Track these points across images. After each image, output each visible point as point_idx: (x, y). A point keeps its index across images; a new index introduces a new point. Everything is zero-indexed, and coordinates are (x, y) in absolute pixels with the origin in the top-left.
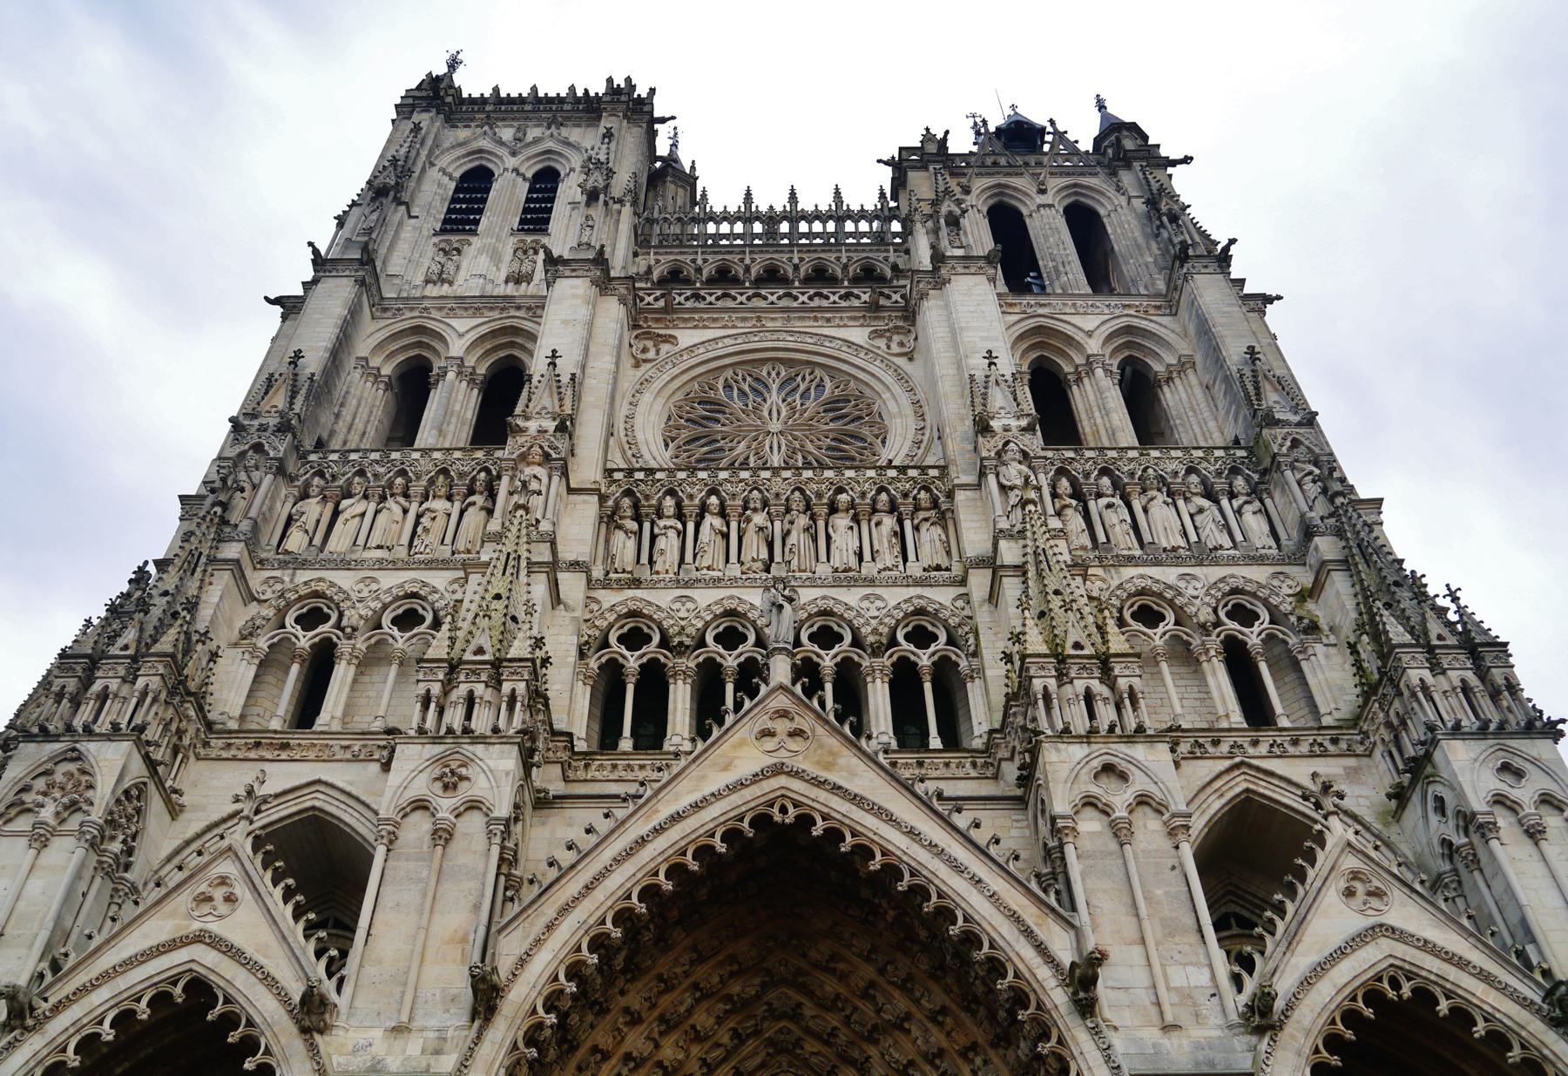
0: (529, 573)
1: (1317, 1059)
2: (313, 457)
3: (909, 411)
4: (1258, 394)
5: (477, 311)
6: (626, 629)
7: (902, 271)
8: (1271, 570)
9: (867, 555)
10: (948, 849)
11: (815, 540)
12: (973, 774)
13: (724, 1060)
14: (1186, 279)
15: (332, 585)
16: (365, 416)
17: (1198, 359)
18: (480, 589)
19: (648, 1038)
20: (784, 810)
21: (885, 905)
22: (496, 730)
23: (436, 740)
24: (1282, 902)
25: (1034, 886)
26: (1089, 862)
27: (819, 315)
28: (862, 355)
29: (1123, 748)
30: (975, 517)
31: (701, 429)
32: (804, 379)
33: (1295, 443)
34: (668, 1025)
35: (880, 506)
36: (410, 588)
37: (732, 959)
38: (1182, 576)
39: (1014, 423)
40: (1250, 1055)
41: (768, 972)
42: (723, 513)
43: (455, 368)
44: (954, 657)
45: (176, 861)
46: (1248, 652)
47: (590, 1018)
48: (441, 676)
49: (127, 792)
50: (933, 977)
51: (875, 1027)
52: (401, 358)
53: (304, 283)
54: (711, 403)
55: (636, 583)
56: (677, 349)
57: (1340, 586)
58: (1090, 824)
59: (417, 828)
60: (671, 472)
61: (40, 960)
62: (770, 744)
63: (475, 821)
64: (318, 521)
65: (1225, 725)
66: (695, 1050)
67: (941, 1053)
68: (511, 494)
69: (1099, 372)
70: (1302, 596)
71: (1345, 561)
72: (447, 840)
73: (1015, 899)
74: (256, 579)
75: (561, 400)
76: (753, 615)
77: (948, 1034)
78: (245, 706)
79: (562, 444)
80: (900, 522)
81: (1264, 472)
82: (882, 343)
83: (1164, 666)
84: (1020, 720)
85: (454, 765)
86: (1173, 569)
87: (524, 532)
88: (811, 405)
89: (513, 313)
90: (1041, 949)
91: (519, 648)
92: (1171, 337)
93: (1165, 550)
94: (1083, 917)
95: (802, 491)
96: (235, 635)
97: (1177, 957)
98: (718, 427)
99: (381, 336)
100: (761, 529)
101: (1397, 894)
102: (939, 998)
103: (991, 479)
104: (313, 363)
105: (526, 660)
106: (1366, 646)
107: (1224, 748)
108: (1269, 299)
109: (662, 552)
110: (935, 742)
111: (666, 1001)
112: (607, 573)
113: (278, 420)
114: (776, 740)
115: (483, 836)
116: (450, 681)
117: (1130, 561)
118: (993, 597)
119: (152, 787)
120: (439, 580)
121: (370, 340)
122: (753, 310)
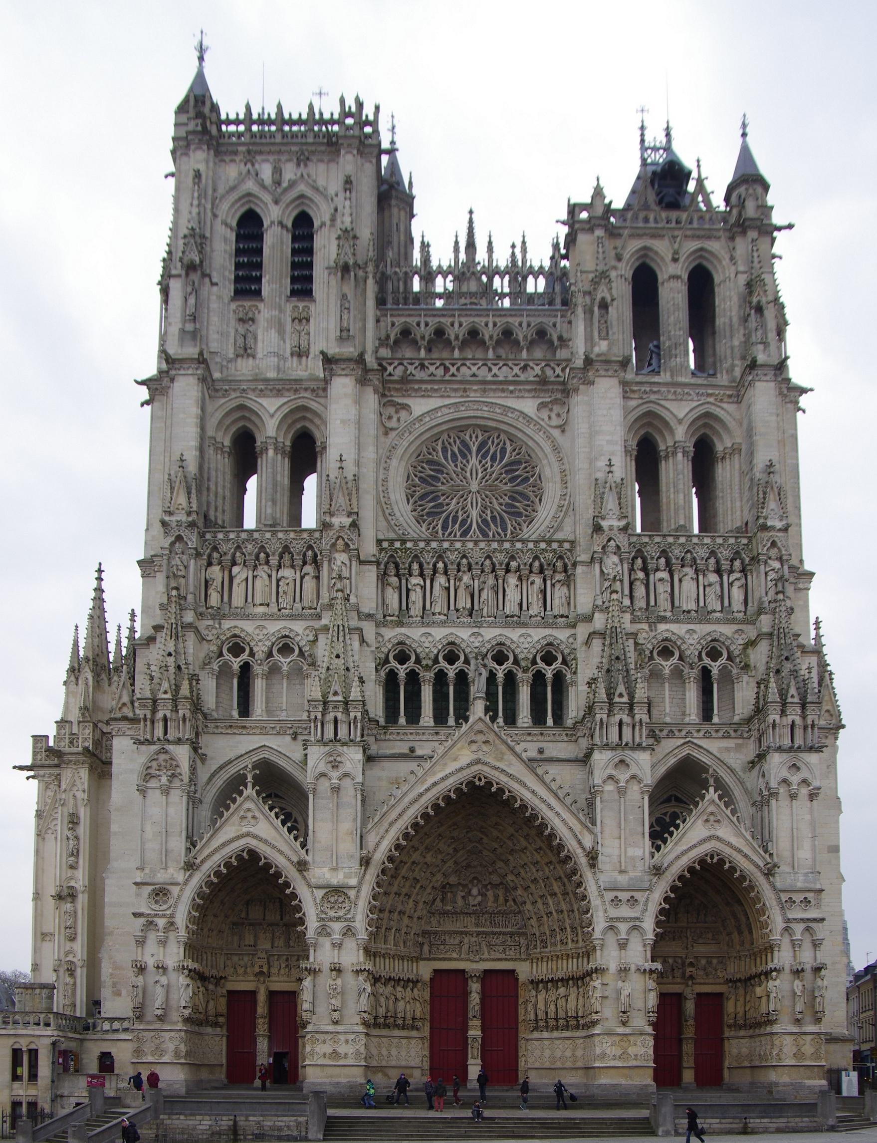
5: (279, 393)
9: (525, 607)
11: (497, 593)
15: (243, 630)
18: (328, 648)
20: (480, 779)
22: (352, 741)
27: (505, 387)
42: (446, 573)
43: (272, 447)
55: (400, 624)
60: (415, 542)
62: (474, 747)
76: (463, 645)
80: (545, 581)
83: (667, 685)
86: (685, 626)
92: (731, 424)
93: (684, 611)
99: (219, 415)
100: (467, 587)
108: (803, 391)
109: (414, 603)
112: (385, 616)
117: (663, 620)
118: (588, 642)
120: (298, 627)
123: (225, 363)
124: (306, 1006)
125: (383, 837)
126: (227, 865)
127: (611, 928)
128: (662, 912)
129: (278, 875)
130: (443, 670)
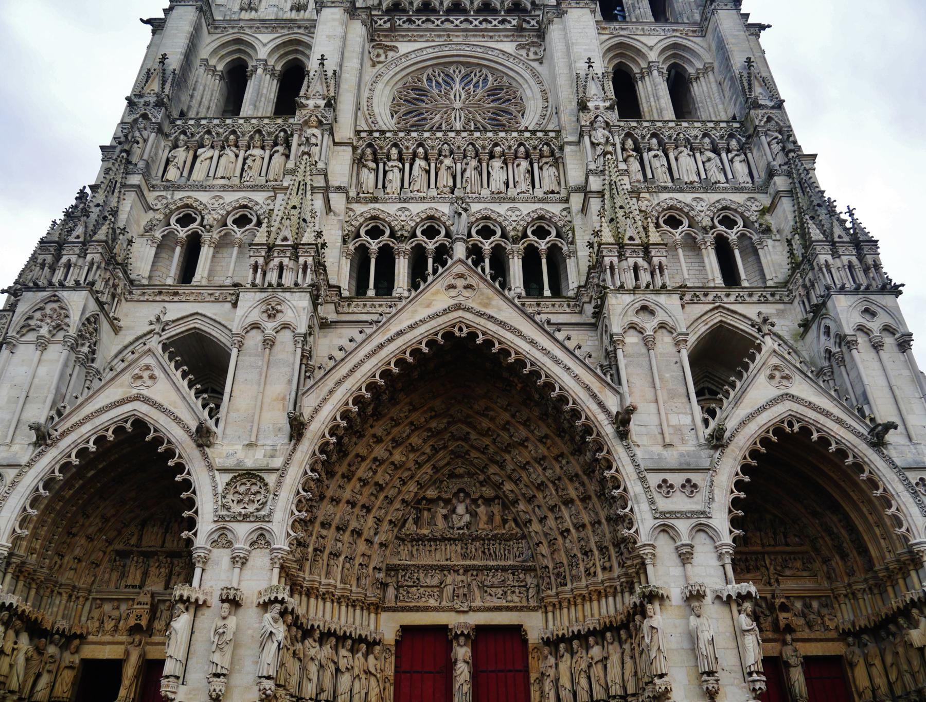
0: (312, 193)
1: (745, 462)
2: (179, 122)
3: (539, 96)
4: (750, 88)
5: (274, 29)
6: (370, 227)
7: (537, 5)
8: (747, 196)
10: (552, 352)
11: (481, 174)
12: (568, 310)
13: (427, 461)
14: (713, 13)
15: (196, 200)
16: (208, 97)
17: (716, 65)
18: (284, 203)
19: (386, 450)
20: (461, 329)
21: (516, 380)
22: (296, 284)
23: (263, 290)
24: (734, 381)
25: (599, 371)
26: (630, 359)
28: (511, 60)
29: (653, 297)
30: (575, 162)
31: (413, 106)
32: (475, 75)
33: (769, 119)
34: (397, 443)
35: (519, 154)
36: (242, 202)
37: (432, 409)
38: (695, 199)
39: (602, 104)
40: (709, 460)
41: (451, 416)
42: (426, 158)
44: (560, 245)
45: (120, 357)
46: (729, 244)
47: (354, 439)
48: (263, 254)
49: (88, 319)
50: (541, 419)
51: (509, 445)
52: (228, 59)
53: (164, 10)
54: (419, 90)
55: (375, 200)
56: (398, 55)
57: (786, 206)
58: (632, 339)
59: (254, 339)
60: (395, 133)
61: (51, 410)
62: (453, 293)
63: (286, 335)
64: (185, 162)
65: (712, 285)
66: (411, 456)
67: (544, 458)
68: (300, 145)
69: (655, 73)
70: (763, 212)
71: (791, 191)
72: (271, 346)
73: (588, 378)
74: (151, 197)
75: (328, 87)
76: (444, 219)
77: (548, 448)
78: (151, 271)
79: (329, 115)
80: (531, 164)
81: (749, 137)
82: (523, 52)
83: (680, 251)
84: (596, 281)
85: (273, 304)
87: (308, 168)
88: (480, 91)
89: (296, 30)
90: (601, 405)
91: (308, 237)
93: (686, 183)
94: (625, 388)
95: (473, 145)
96: (142, 230)
97: (674, 409)
98: (424, 105)
100: (449, 168)
101: (797, 378)
102: (545, 430)
103: (586, 138)
104: (174, 62)
105: (313, 244)
106: (797, 241)
107: (710, 298)
108: (762, 27)
109: (390, 181)
110: (547, 292)
111: (395, 431)
112: (358, 194)
113: (155, 99)
114: (457, 290)
115: (292, 343)
116: (268, 256)
117: (665, 189)
118: (584, 210)
119: (102, 317)
120: (259, 197)
121: (208, 48)
122: (445, 30)
123: (229, 13)
124: (169, 668)
125: (325, 400)
126: (100, 440)
127: (665, 529)
128: (736, 503)
129: (170, 453)
130: (421, 245)
